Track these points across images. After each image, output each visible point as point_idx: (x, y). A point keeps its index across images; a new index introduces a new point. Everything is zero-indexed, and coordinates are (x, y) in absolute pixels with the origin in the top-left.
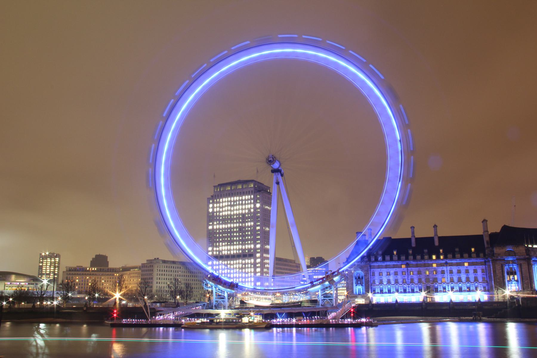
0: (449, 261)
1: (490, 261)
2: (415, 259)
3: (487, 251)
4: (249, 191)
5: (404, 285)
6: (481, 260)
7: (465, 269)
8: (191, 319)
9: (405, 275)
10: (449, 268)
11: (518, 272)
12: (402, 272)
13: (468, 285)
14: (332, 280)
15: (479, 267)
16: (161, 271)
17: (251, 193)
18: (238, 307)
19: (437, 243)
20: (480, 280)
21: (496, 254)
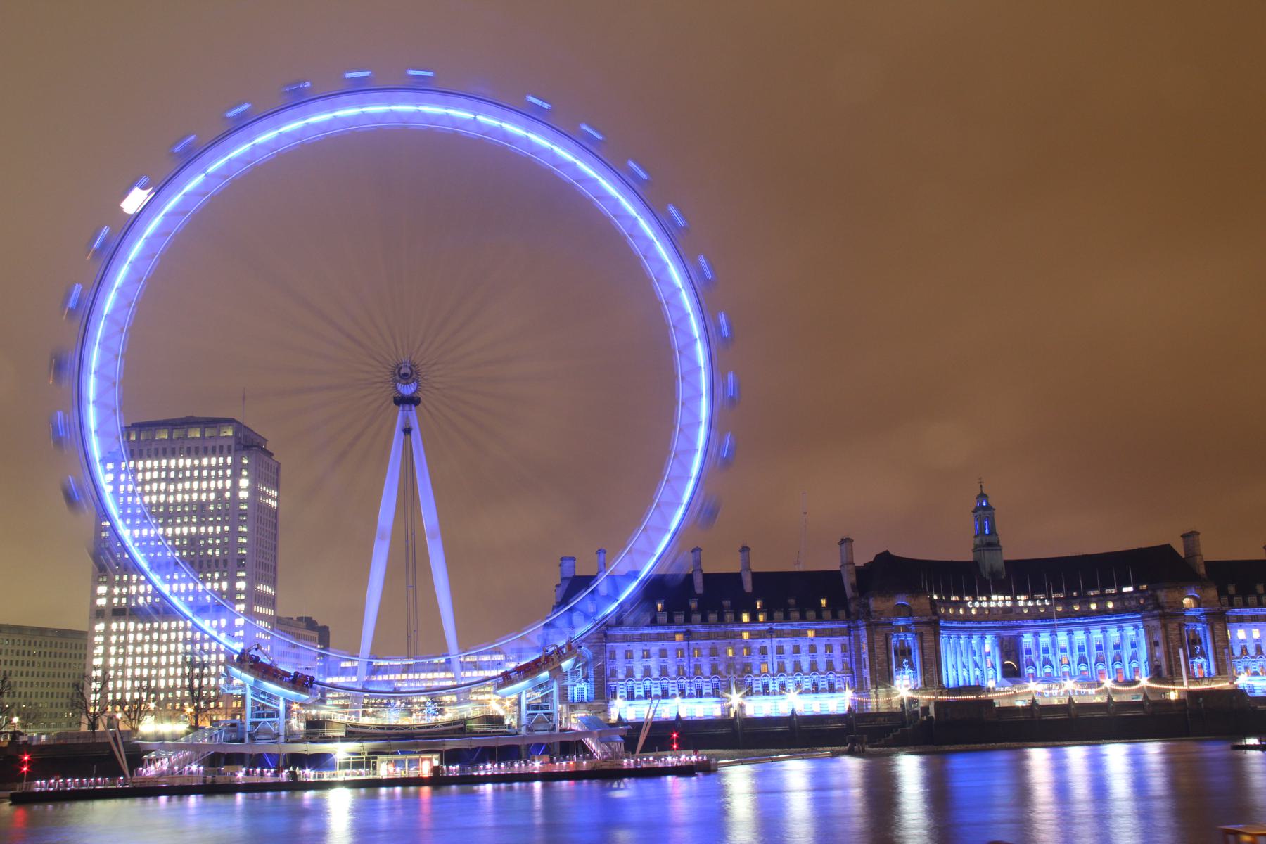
0: (777, 625)
2: (704, 621)
3: (853, 607)
4: (221, 447)
5: (681, 680)
7: (808, 644)
8: (251, 770)
9: (682, 656)
10: (776, 641)
11: (917, 651)
12: (677, 650)
15: (837, 640)
17: (225, 450)
19: (748, 587)
20: (839, 667)
21: (875, 612)
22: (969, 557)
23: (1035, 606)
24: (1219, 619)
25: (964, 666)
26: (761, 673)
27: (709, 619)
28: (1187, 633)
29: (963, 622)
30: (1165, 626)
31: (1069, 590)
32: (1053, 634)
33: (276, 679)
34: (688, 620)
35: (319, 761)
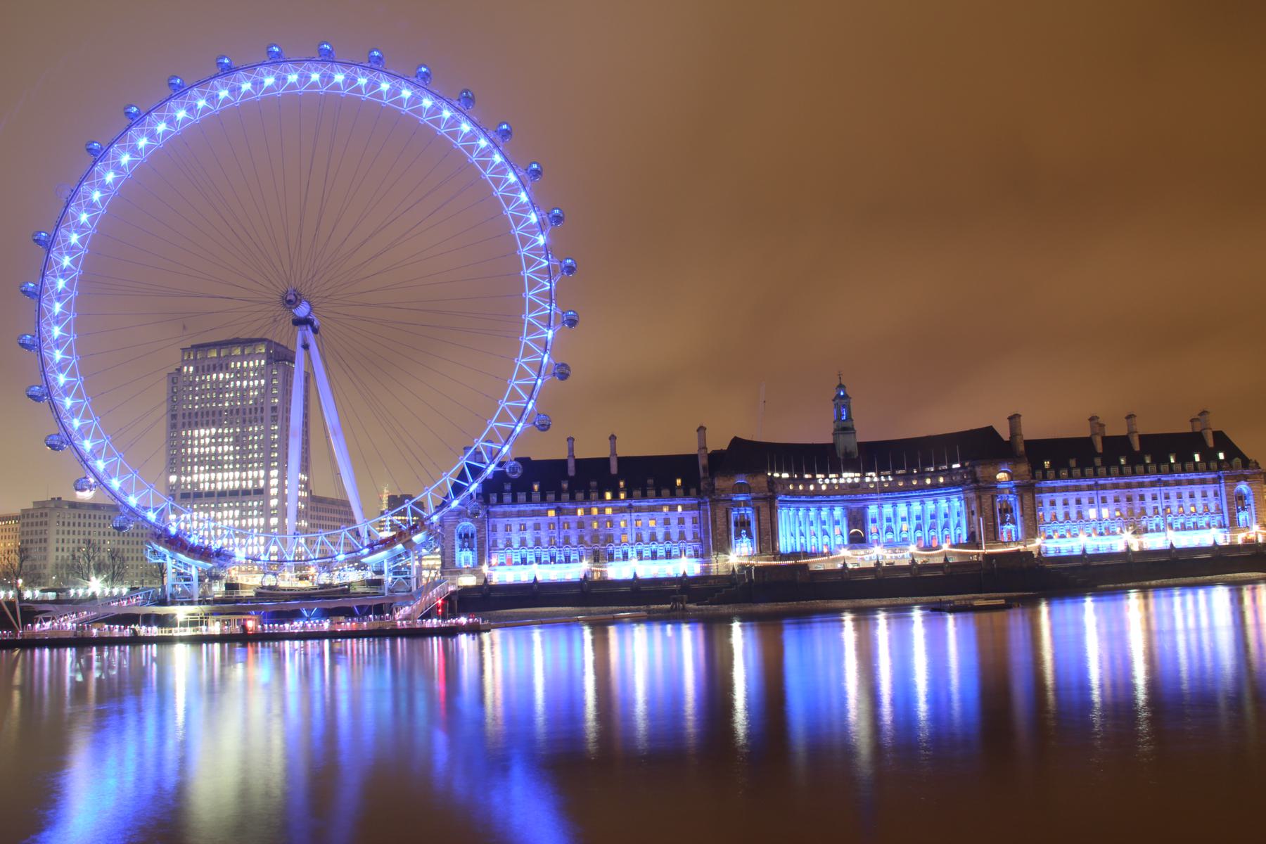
0: (635, 502)
1: (706, 502)
3: (703, 485)
6: (691, 500)
8: (112, 626)
9: (554, 529)
10: (634, 515)
12: (549, 524)
13: (668, 546)
14: (411, 540)
16: (66, 524)
18: (221, 596)
19: (614, 469)
20: (689, 537)
21: (718, 489)
22: (831, 442)
23: (880, 482)
24: (1028, 490)
25: (792, 535)
26: (621, 542)
27: (576, 498)
28: (1001, 504)
29: (812, 497)
30: (979, 498)
31: (911, 466)
32: (894, 505)
33: (185, 551)
34: (558, 499)
35: (163, 621)
